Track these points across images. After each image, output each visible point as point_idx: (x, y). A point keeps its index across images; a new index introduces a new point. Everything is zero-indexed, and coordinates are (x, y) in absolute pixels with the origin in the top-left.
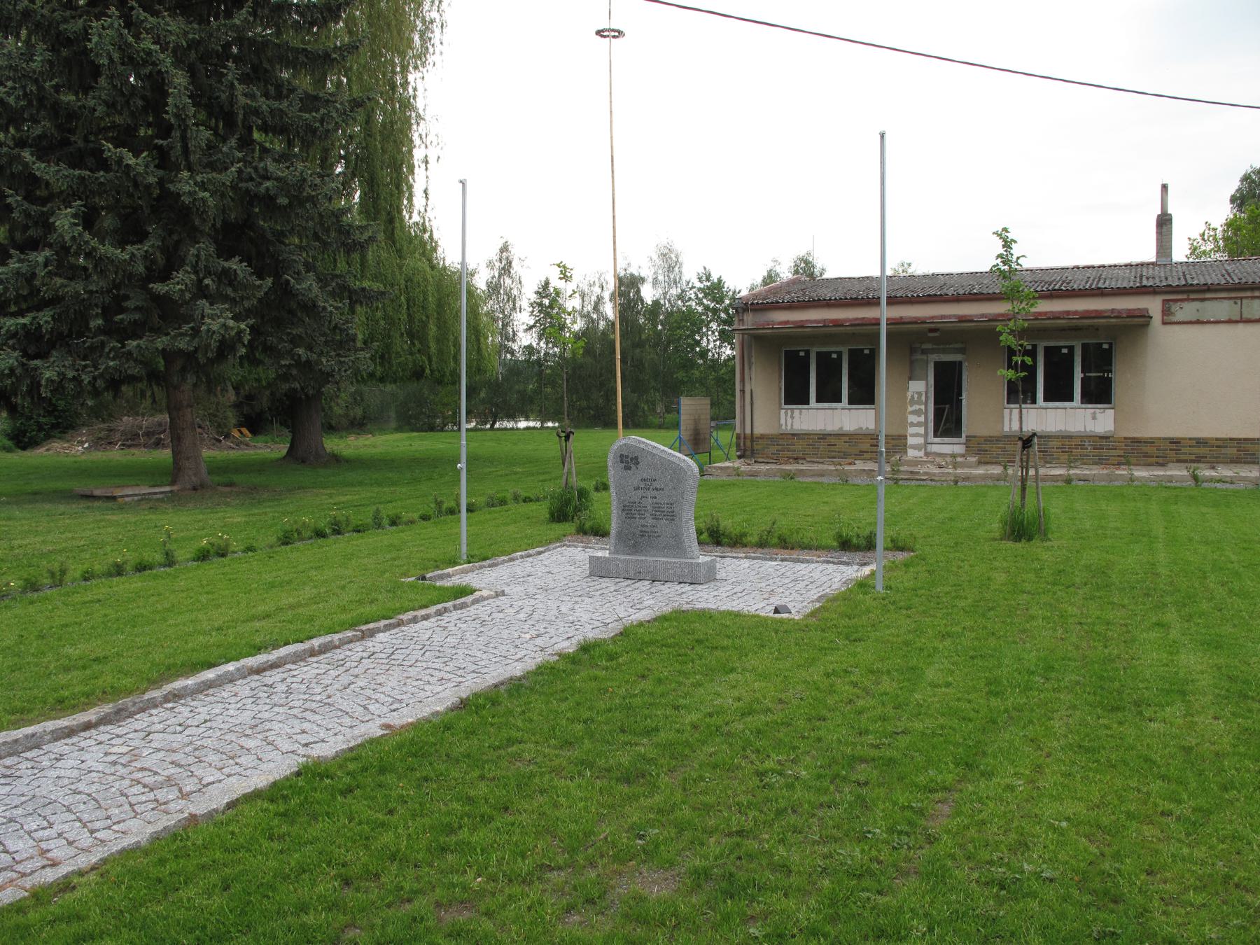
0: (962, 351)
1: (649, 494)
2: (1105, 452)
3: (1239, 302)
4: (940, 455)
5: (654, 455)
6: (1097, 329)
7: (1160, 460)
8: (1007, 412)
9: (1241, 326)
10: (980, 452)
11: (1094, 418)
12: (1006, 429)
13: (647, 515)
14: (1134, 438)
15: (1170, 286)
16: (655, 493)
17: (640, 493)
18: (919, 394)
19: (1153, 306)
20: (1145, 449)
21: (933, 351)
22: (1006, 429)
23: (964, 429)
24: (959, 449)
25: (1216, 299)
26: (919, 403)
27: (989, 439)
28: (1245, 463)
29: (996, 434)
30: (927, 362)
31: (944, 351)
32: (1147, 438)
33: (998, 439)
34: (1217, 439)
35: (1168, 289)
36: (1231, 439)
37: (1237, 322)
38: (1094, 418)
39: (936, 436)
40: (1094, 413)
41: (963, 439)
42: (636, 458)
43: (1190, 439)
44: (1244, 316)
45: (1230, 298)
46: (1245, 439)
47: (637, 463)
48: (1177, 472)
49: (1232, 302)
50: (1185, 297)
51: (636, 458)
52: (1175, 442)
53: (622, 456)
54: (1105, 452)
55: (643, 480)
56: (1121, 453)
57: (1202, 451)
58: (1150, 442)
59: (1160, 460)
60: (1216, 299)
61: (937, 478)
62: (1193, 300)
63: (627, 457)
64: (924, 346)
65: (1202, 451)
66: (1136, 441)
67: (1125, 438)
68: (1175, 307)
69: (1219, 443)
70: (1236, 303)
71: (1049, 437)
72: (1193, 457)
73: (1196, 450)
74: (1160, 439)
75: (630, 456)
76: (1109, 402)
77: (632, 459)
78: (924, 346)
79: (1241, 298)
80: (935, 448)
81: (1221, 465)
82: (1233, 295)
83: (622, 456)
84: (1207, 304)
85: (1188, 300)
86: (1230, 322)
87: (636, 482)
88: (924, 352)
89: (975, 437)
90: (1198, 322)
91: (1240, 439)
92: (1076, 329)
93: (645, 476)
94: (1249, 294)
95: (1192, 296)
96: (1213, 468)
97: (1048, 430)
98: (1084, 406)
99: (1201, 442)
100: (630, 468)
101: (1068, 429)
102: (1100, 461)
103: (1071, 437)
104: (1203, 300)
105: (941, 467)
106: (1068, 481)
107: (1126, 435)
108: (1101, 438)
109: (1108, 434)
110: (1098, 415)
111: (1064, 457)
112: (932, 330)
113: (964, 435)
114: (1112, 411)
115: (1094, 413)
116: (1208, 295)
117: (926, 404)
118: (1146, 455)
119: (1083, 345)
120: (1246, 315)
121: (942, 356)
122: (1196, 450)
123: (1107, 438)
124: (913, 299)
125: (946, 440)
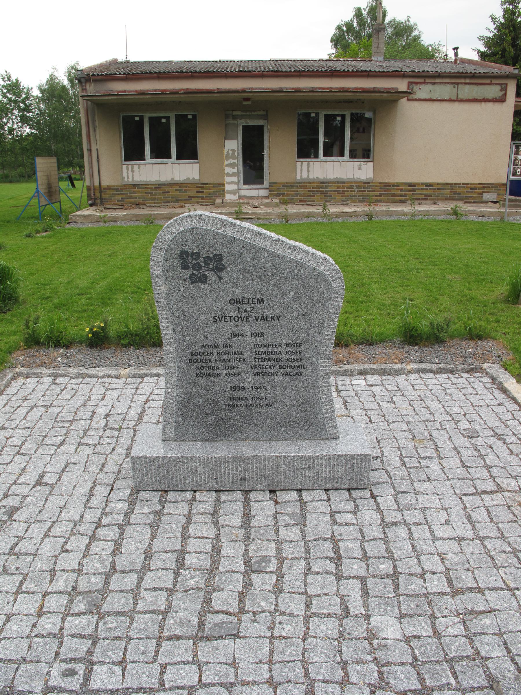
0: (265, 117)
1: (247, 328)
2: (366, 193)
3: (456, 86)
4: (249, 198)
5: (259, 249)
6: (363, 103)
7: (403, 199)
8: (299, 164)
9: (456, 104)
10: (279, 195)
11: (360, 169)
12: (298, 177)
13: (242, 367)
14: (386, 183)
15: (414, 71)
16: (261, 326)
17: (228, 327)
18: (233, 151)
19: (402, 85)
20: (393, 191)
21: (241, 117)
22: (298, 177)
23: (266, 177)
24: (263, 193)
25: (443, 83)
26: (233, 157)
27: (286, 185)
28: (454, 200)
29: (291, 181)
30: (237, 126)
31: (250, 117)
32: (394, 183)
33: (292, 185)
34: (438, 184)
35: (414, 74)
36: (447, 184)
37: (454, 101)
38: (360, 169)
39: (245, 183)
40: (360, 165)
41: (266, 184)
42: (218, 258)
43: (422, 184)
44: (459, 97)
45: (451, 83)
46: (455, 184)
47: (221, 268)
48: (445, 207)
49: (452, 86)
50: (422, 80)
51: (218, 258)
52: (412, 185)
53: (183, 255)
54: (366, 193)
55: (235, 301)
56: (377, 194)
57: (428, 192)
58: (396, 186)
59: (403, 199)
60: (443, 83)
61: (262, 217)
62: (428, 83)
63: (196, 256)
64: (235, 113)
65: (428, 192)
66: (387, 185)
67: (380, 183)
68: (416, 88)
69: (440, 186)
70: (454, 87)
71: (329, 183)
72: (423, 196)
73: (425, 192)
74: (402, 183)
75: (204, 253)
76: (368, 157)
77: (208, 260)
78: (235, 113)
79: (458, 84)
80: (245, 193)
81: (440, 202)
82: (453, 81)
83: (183, 255)
84: (437, 87)
85: (424, 83)
86: (450, 100)
87: (218, 308)
88: (235, 117)
89: (276, 183)
90: (430, 100)
91: (452, 184)
92: (349, 102)
93: (238, 293)
94: (463, 81)
95: (427, 80)
96: (435, 204)
97: (328, 178)
98: (351, 160)
99: (428, 186)
100: (203, 279)
101: (342, 177)
102: (364, 200)
103: (344, 183)
104: (434, 83)
105: (255, 207)
106: (370, 216)
107: (382, 181)
108: (365, 183)
109: (369, 181)
110: (362, 167)
111: (339, 197)
112: (247, 99)
113: (265, 182)
114: (372, 163)
115: (360, 165)
116: (437, 80)
117: (237, 158)
118: (394, 195)
119: (352, 114)
120: (460, 97)
121: (248, 120)
122: (425, 192)
123: (369, 183)
124: (228, 74)
125: (252, 186)
